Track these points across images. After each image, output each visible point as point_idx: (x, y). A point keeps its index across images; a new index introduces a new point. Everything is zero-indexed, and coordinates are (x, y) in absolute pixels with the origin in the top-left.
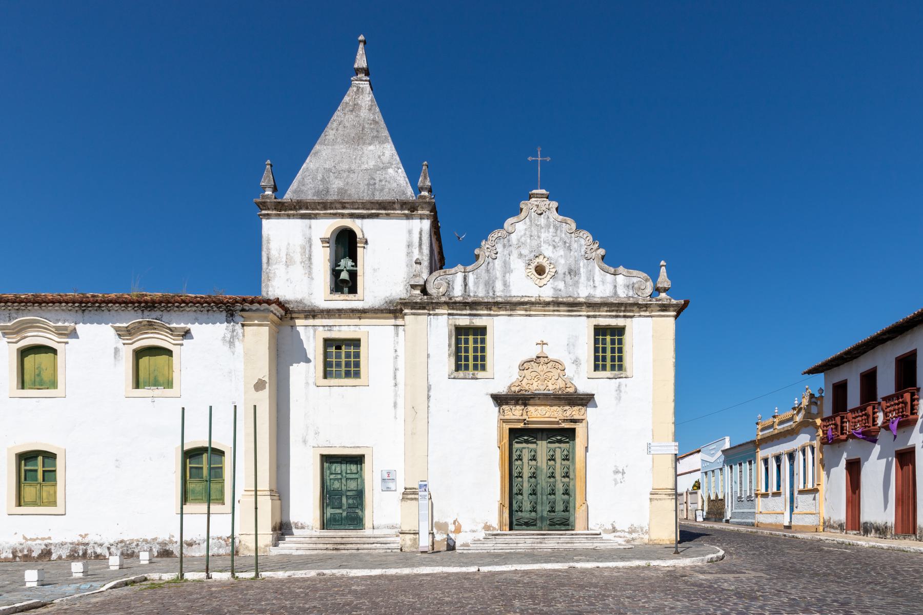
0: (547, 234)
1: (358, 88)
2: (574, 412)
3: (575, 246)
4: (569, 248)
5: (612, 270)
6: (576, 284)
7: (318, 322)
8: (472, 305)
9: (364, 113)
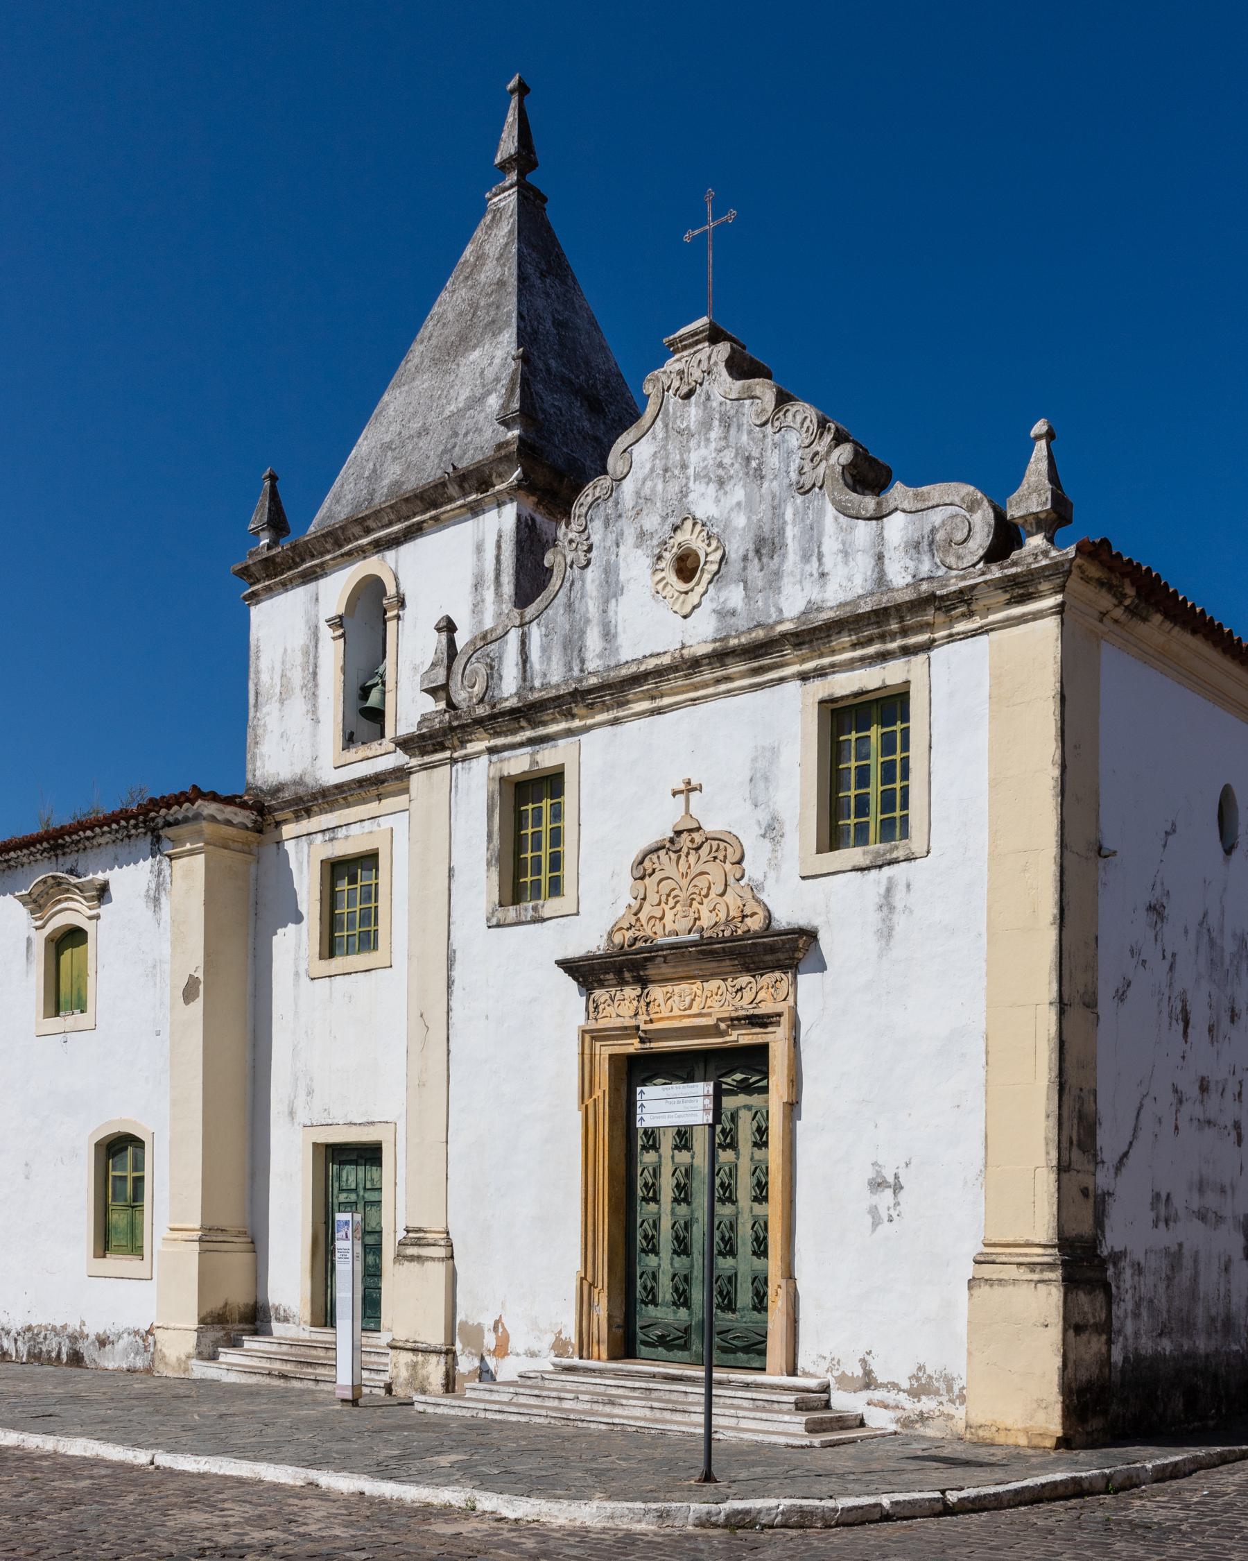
0: (703, 451)
2: (763, 992)
3: (773, 460)
4: (759, 475)
5: (869, 502)
6: (774, 580)
8: (528, 713)
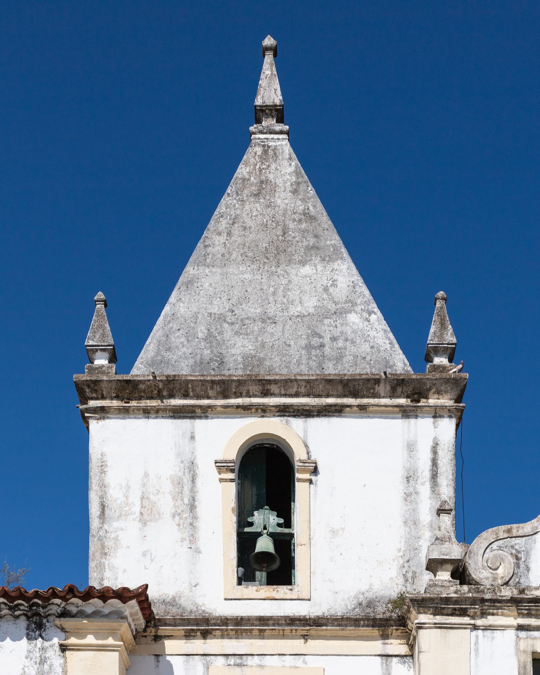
1: (266, 149)
7: (214, 645)
9: (283, 199)
